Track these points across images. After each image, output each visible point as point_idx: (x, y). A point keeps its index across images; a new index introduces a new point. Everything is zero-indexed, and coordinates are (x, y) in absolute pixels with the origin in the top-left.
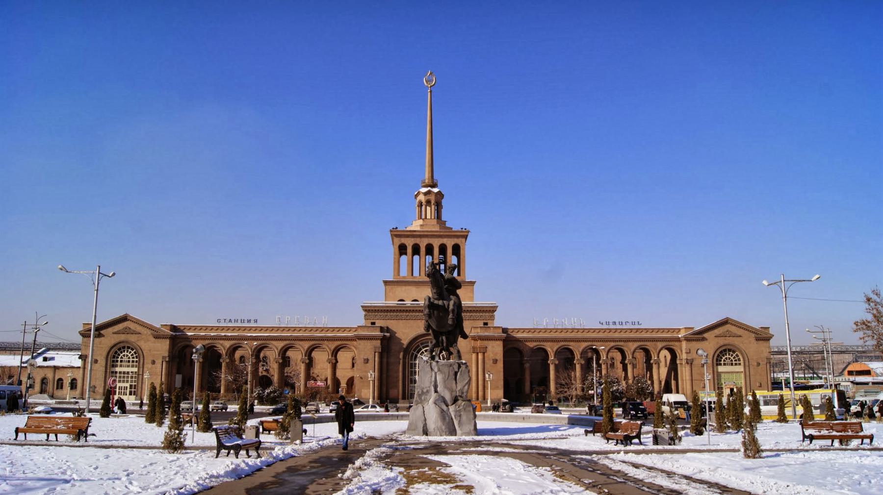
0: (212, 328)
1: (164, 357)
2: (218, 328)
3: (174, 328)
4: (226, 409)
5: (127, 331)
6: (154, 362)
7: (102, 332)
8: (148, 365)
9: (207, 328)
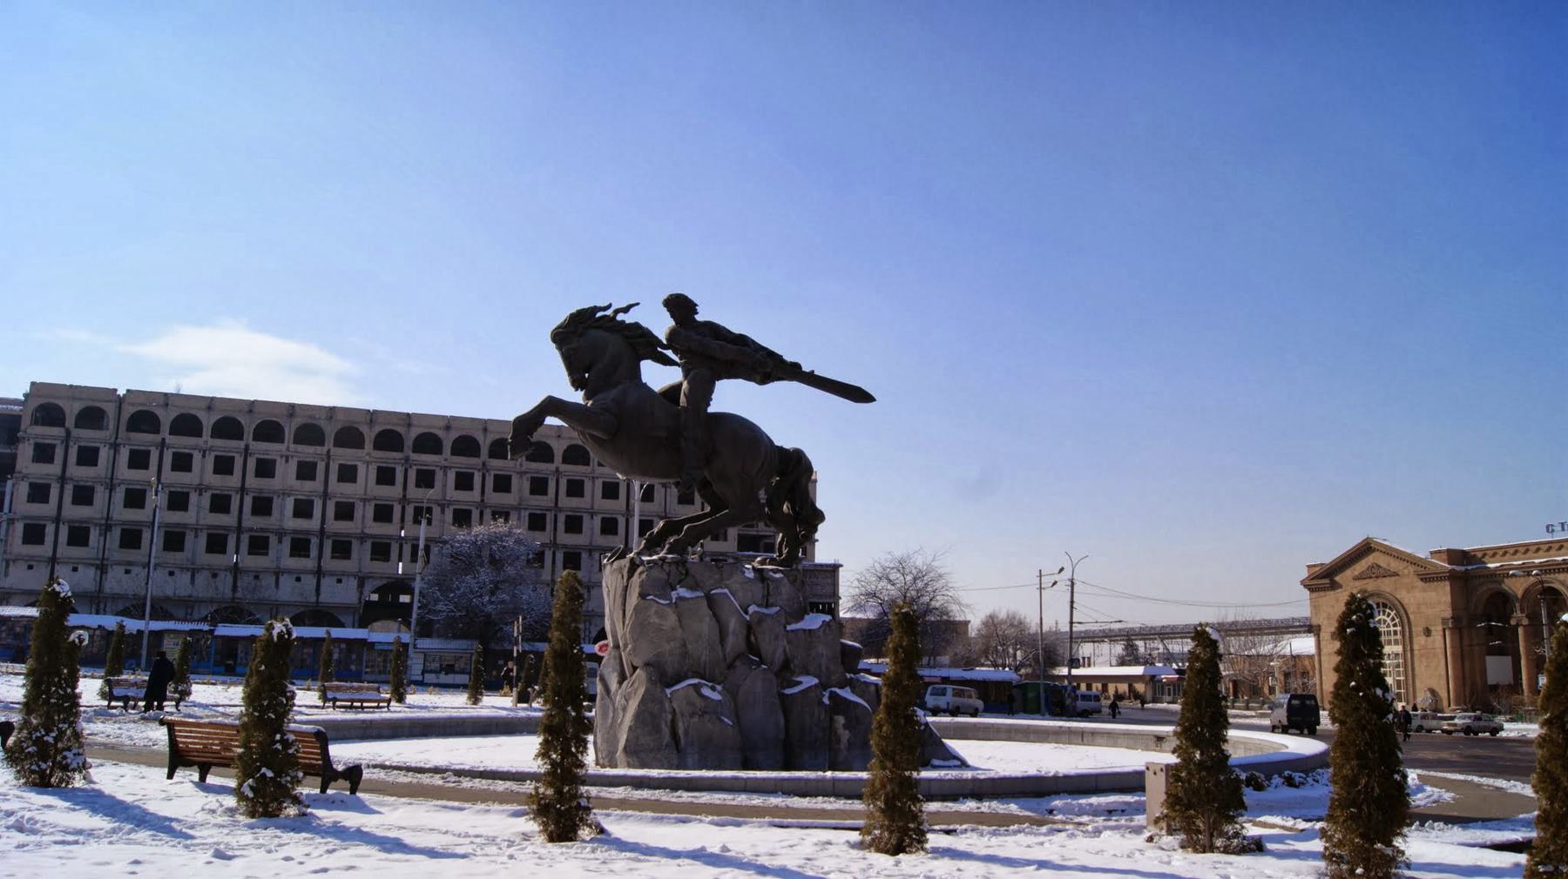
0: (1538, 548)
1: (1444, 621)
2: (1549, 546)
3: (1458, 556)
4: (1496, 730)
5: (1376, 572)
6: (1428, 632)
7: (1337, 579)
8: (1419, 640)
9: (1526, 549)
